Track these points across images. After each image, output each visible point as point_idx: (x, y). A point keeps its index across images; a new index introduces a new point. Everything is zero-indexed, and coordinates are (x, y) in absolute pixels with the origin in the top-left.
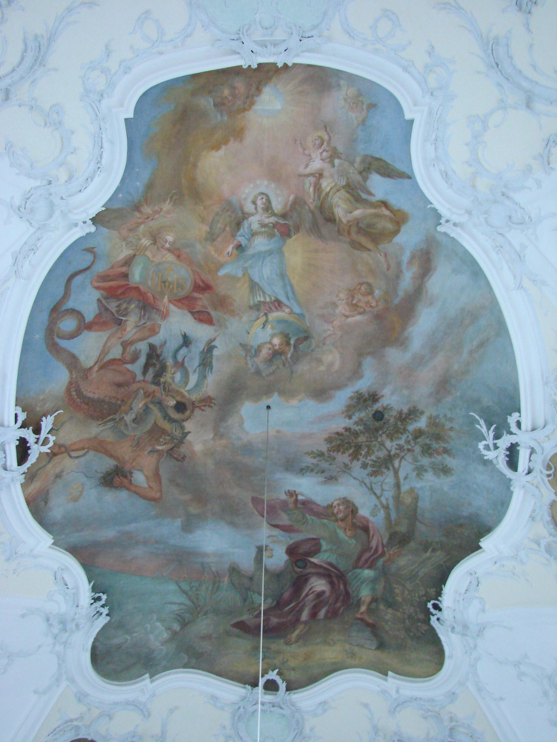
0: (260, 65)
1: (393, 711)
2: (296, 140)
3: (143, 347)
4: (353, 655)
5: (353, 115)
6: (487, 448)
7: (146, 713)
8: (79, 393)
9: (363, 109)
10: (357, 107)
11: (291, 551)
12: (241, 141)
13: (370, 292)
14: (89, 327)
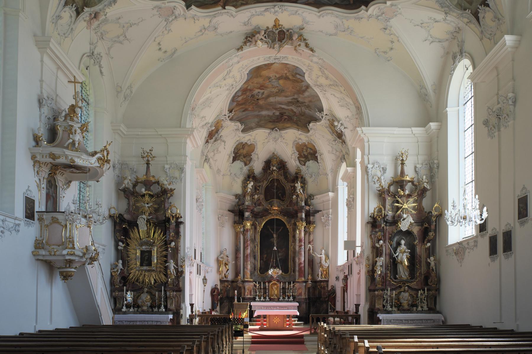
1: (299, 135)
3: (250, 95)
4: (292, 126)
6: (318, 114)
7: (251, 136)
8: (238, 104)
11: (280, 113)
13: (296, 87)
14: (240, 96)
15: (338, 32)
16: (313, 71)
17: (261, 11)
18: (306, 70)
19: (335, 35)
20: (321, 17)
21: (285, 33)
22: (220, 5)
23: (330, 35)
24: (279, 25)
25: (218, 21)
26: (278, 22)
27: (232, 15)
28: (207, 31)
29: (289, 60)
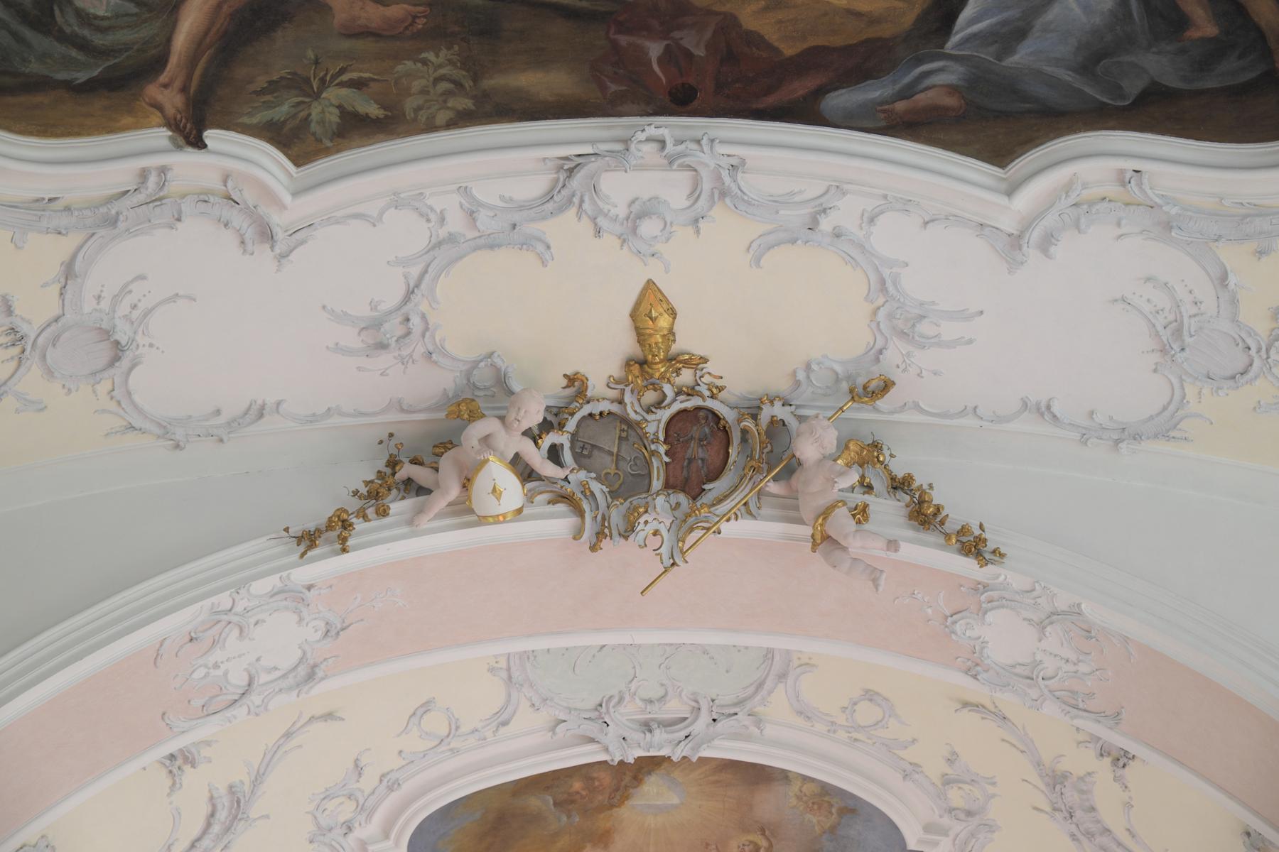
0: (639, 759)
2: (707, 845)
5: (815, 820)
9: (831, 813)
10: (819, 808)
12: (606, 846)
15: (1191, 391)
16: (991, 828)
17: (521, 207)
18: (928, 828)
19: (1164, 434)
20: (1032, 254)
21: (726, 431)
22: (159, 107)
23: (1125, 435)
24: (671, 359)
25: (142, 277)
26: (664, 322)
27: (267, 234)
28: (34, 371)
29: (769, 731)
